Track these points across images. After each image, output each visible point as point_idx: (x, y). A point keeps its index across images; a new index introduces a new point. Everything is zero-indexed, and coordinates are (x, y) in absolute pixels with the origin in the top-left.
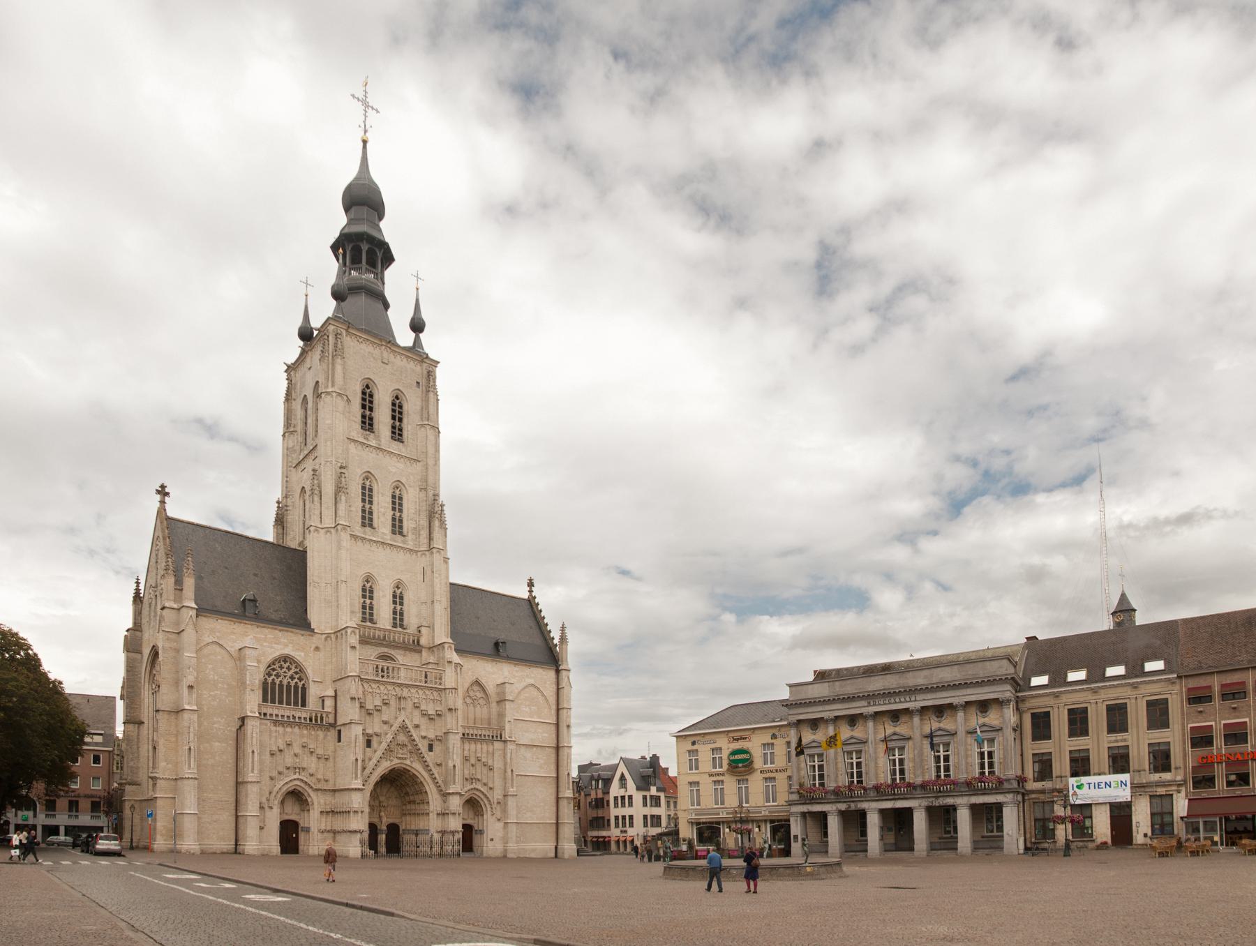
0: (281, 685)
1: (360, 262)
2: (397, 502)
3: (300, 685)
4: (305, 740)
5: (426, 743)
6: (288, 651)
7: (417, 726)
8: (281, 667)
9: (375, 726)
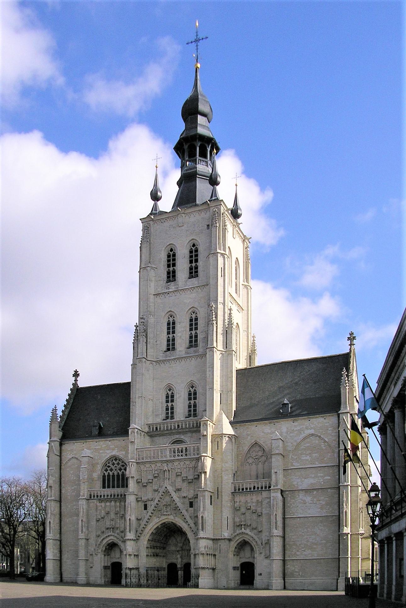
0: (113, 476)
4: (118, 509)
6: (115, 453)
7: (179, 490)
8: (113, 464)
9: (148, 494)
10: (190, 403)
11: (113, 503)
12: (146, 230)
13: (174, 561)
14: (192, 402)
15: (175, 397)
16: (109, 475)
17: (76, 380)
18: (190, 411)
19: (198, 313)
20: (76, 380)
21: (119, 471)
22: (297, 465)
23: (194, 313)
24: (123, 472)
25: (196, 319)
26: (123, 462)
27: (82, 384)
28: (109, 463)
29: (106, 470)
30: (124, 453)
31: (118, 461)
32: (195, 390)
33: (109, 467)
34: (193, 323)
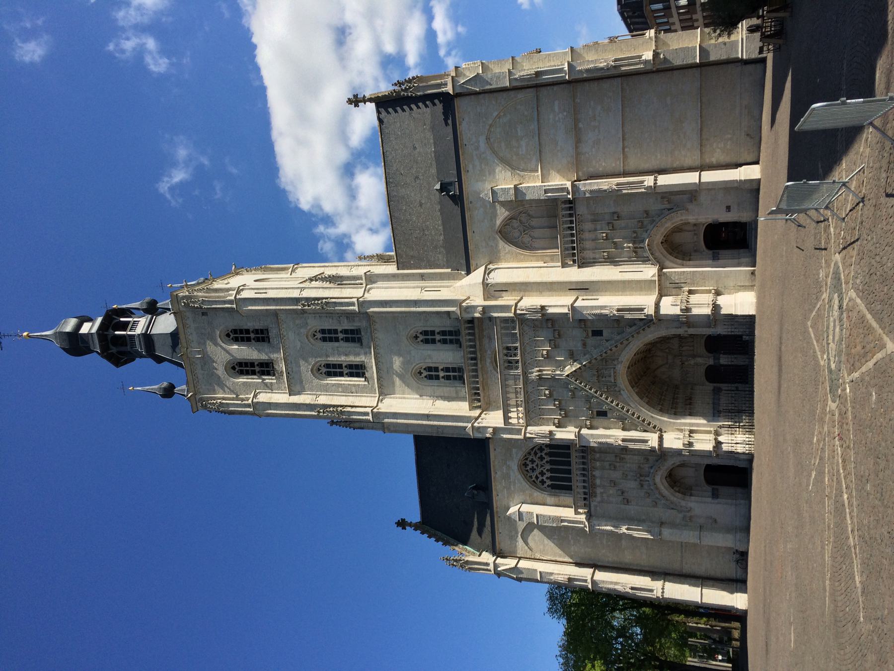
3: (547, 450)
4: (607, 464)
8: (533, 469)
10: (439, 341)
11: (597, 473)
13: (702, 370)
14: (438, 337)
15: (431, 365)
16: (551, 478)
17: (410, 525)
18: (451, 342)
19: (314, 329)
21: (544, 461)
24: (546, 454)
25: (323, 331)
26: (529, 453)
27: (415, 516)
28: (531, 477)
29: (543, 482)
30: (514, 451)
31: (528, 462)
32: (421, 333)
33: (537, 477)
34: (329, 336)
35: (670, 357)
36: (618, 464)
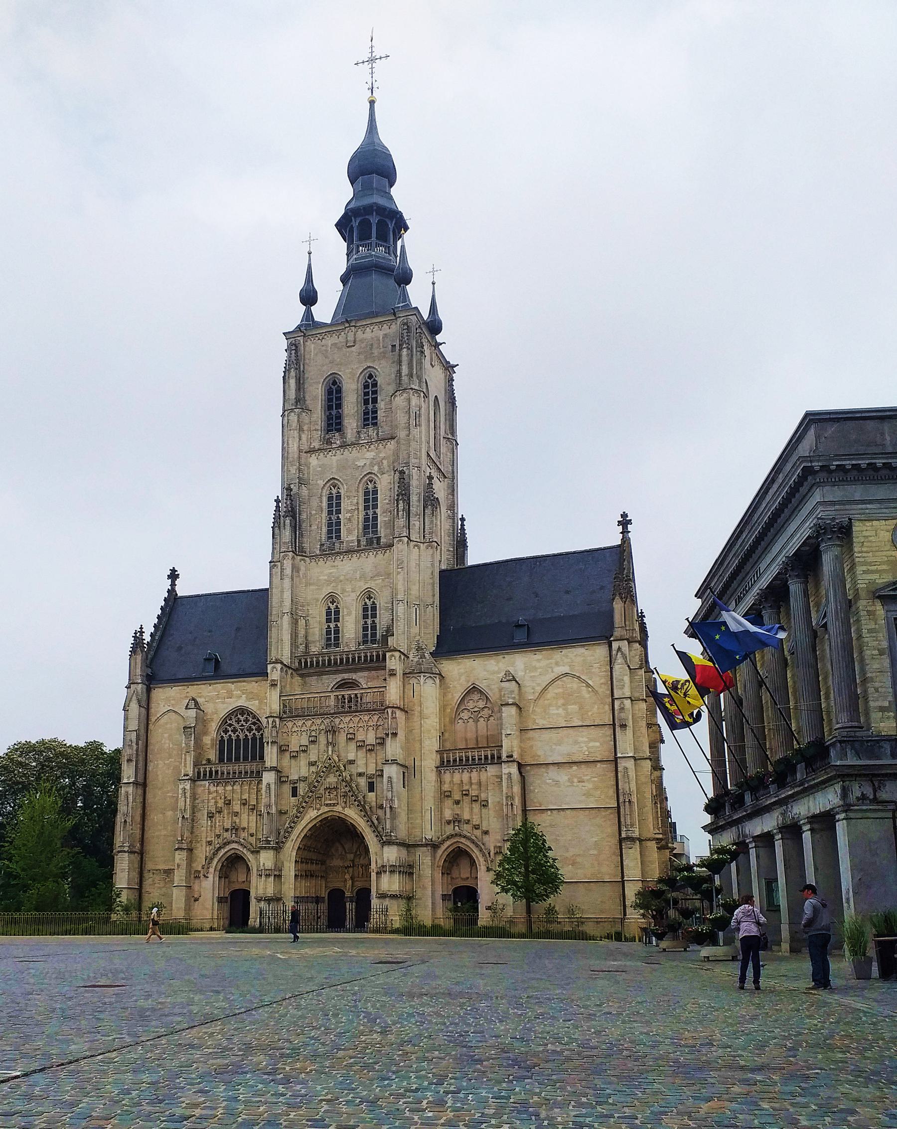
1: (370, 237)
2: (370, 498)
3: (258, 735)
5: (363, 782)
6: (242, 702)
8: (238, 721)
12: (294, 349)
13: (338, 885)
17: (173, 585)
20: (173, 585)
22: (542, 723)
23: (371, 481)
25: (375, 492)
26: (254, 717)
27: (182, 590)
28: (231, 719)
29: (226, 731)
33: (230, 725)
35: (352, 856)
36: (247, 807)
